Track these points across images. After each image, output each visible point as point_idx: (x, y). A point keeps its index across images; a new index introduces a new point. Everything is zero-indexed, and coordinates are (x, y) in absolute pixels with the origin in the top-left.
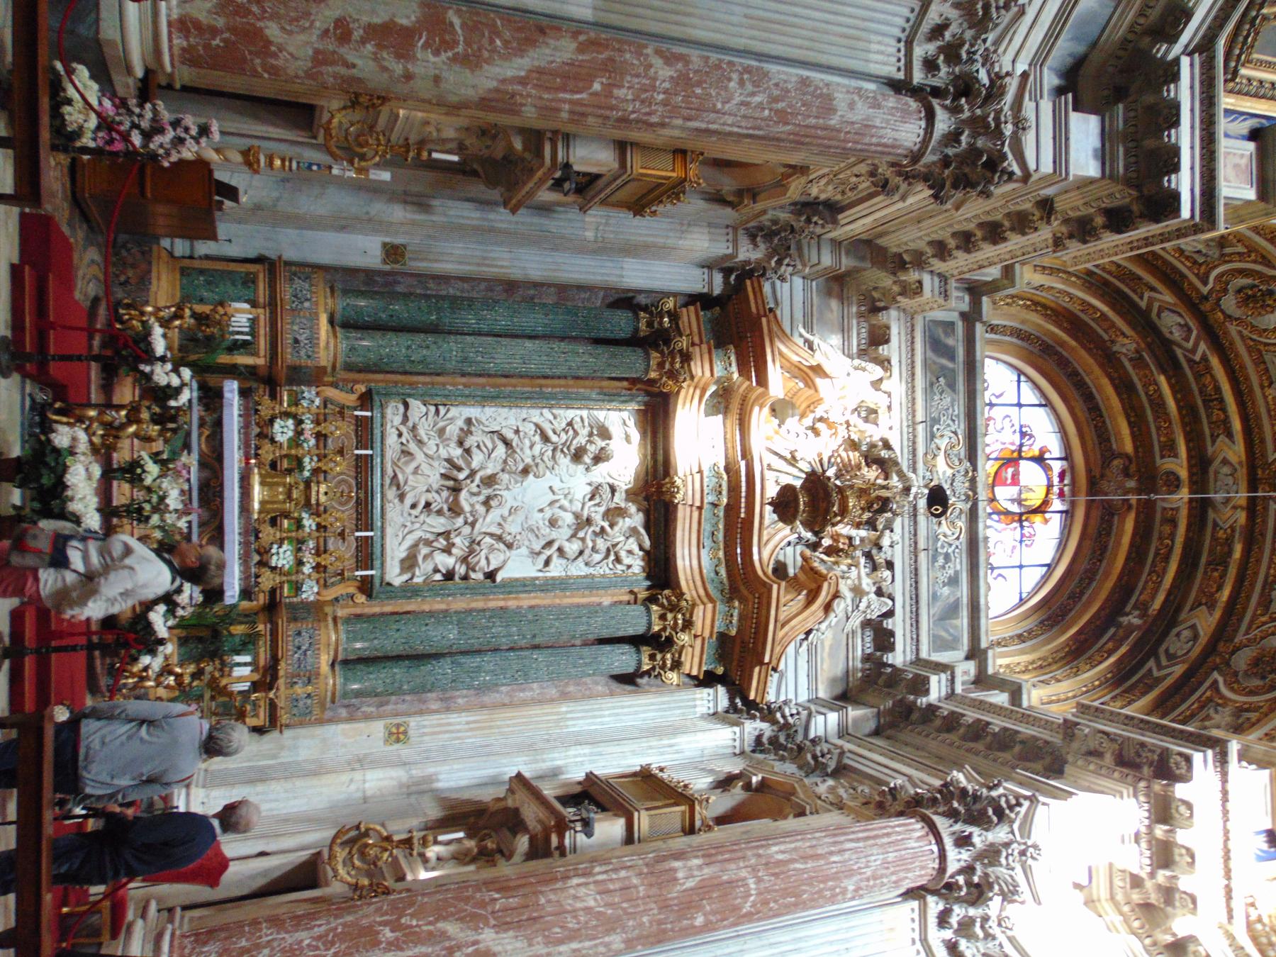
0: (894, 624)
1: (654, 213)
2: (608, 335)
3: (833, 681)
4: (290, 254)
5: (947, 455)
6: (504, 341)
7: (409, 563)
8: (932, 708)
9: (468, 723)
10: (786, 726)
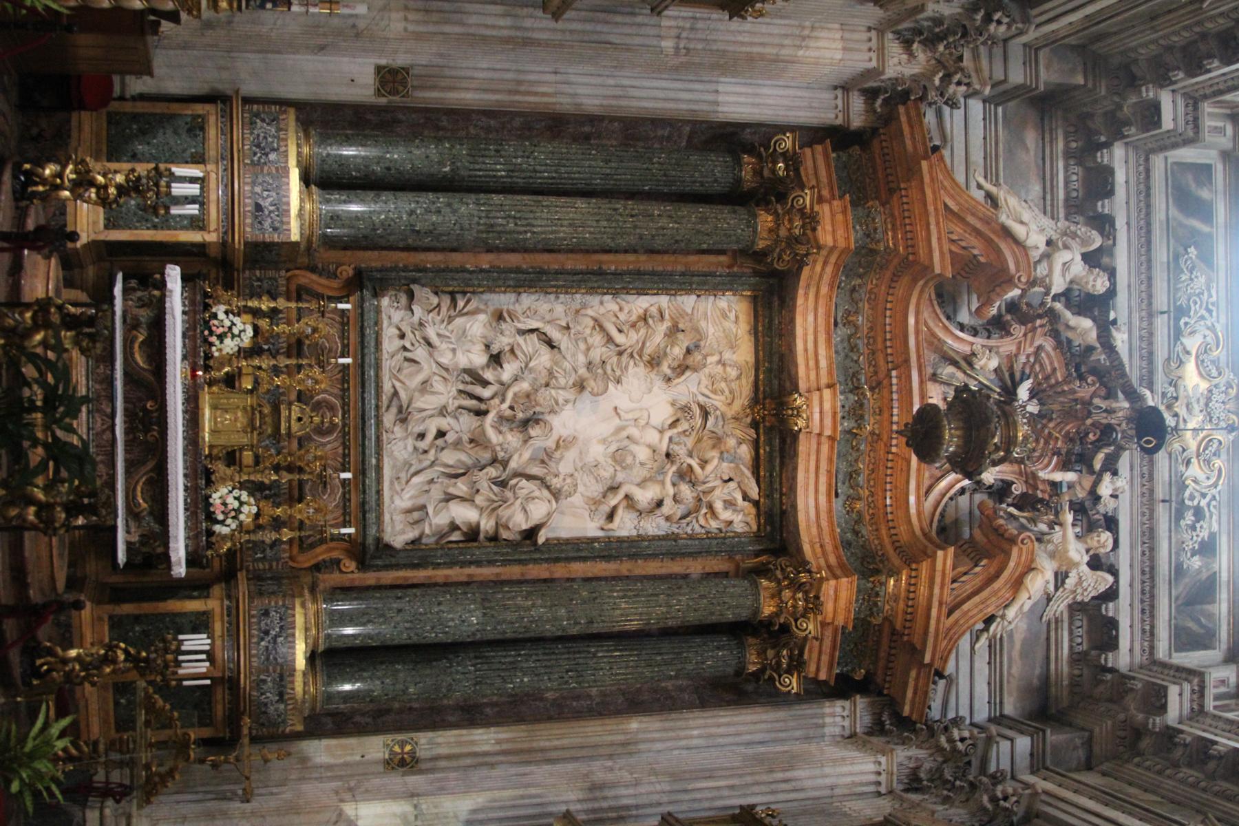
0: (1117, 610)
1: (761, 14)
2: (697, 187)
4: (251, 88)
5: (1200, 363)
9: (498, 742)
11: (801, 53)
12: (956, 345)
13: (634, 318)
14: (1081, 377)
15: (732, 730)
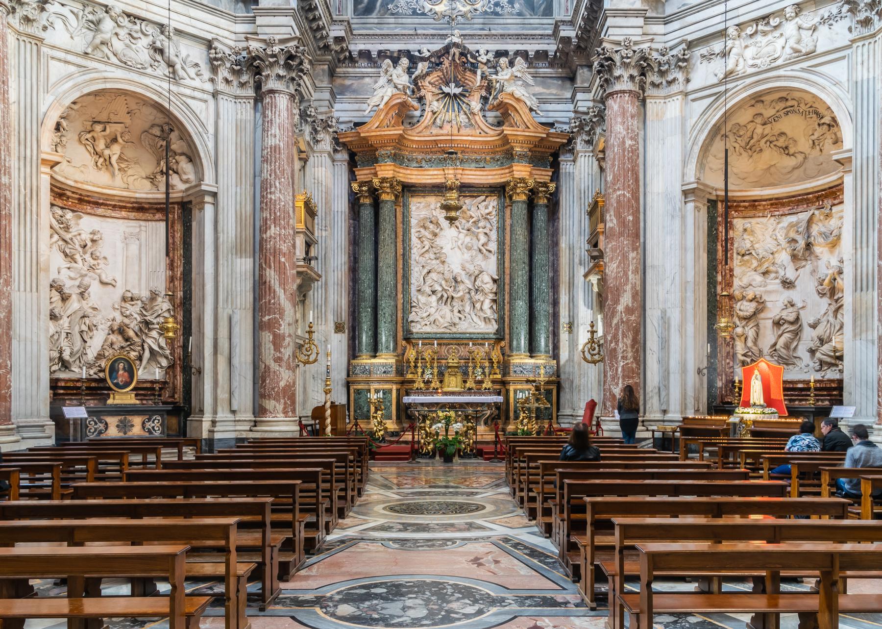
0: (532, 51)
2: (373, 220)
3: (562, 88)
6: (380, 276)
7: (486, 320)
8: (577, 35)
10: (581, 127)
11: (324, 184)
12: (429, 117)
13: (419, 242)
14: (441, 63)
15: (568, 209)
